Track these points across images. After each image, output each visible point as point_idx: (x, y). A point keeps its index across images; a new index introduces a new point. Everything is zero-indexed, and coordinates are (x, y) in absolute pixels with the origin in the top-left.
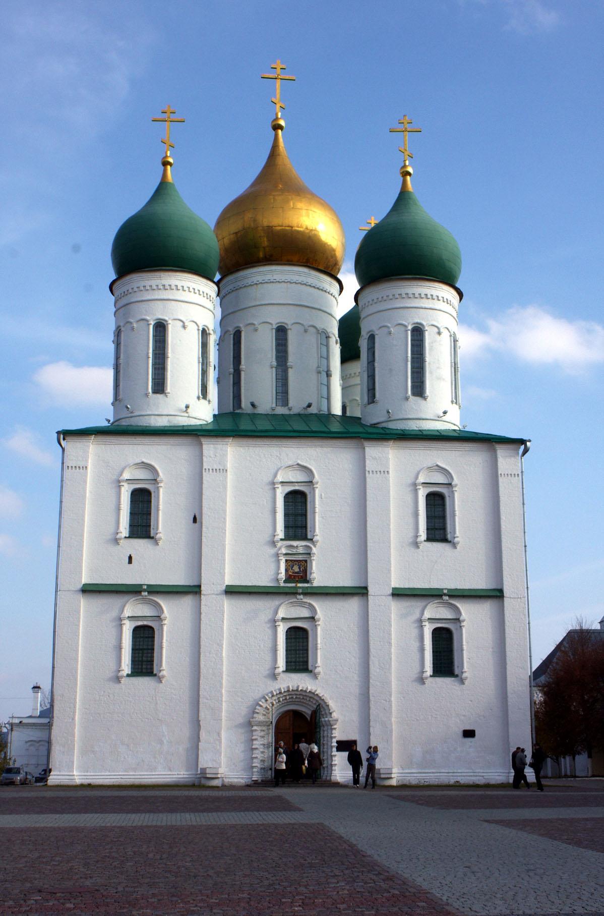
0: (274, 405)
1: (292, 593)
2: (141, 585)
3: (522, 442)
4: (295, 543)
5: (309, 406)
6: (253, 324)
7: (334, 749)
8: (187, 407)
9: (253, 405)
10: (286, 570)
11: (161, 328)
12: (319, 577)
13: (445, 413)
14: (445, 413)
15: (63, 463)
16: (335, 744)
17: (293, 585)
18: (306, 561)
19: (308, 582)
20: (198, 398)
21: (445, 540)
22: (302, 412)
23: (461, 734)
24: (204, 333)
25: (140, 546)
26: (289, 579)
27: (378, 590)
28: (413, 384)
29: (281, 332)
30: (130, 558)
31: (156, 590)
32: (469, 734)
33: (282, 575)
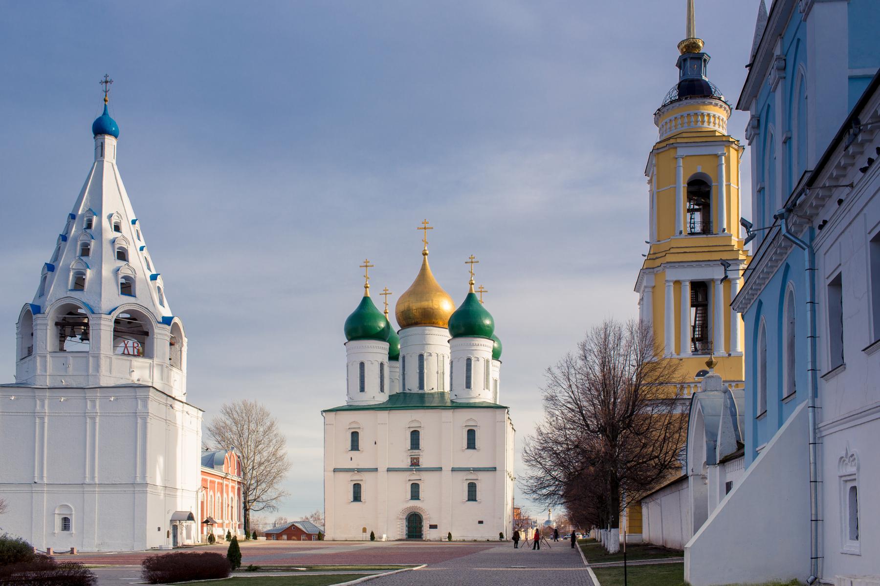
1: (411, 470)
2: (354, 469)
3: (506, 408)
4: (414, 451)
8: (374, 397)
10: (411, 462)
11: (362, 365)
12: (424, 463)
17: (413, 467)
19: (419, 466)
20: (379, 392)
21: (474, 448)
24: (382, 365)
25: (354, 454)
26: (412, 465)
27: (447, 468)
30: (351, 458)
31: (359, 470)
32: (481, 522)
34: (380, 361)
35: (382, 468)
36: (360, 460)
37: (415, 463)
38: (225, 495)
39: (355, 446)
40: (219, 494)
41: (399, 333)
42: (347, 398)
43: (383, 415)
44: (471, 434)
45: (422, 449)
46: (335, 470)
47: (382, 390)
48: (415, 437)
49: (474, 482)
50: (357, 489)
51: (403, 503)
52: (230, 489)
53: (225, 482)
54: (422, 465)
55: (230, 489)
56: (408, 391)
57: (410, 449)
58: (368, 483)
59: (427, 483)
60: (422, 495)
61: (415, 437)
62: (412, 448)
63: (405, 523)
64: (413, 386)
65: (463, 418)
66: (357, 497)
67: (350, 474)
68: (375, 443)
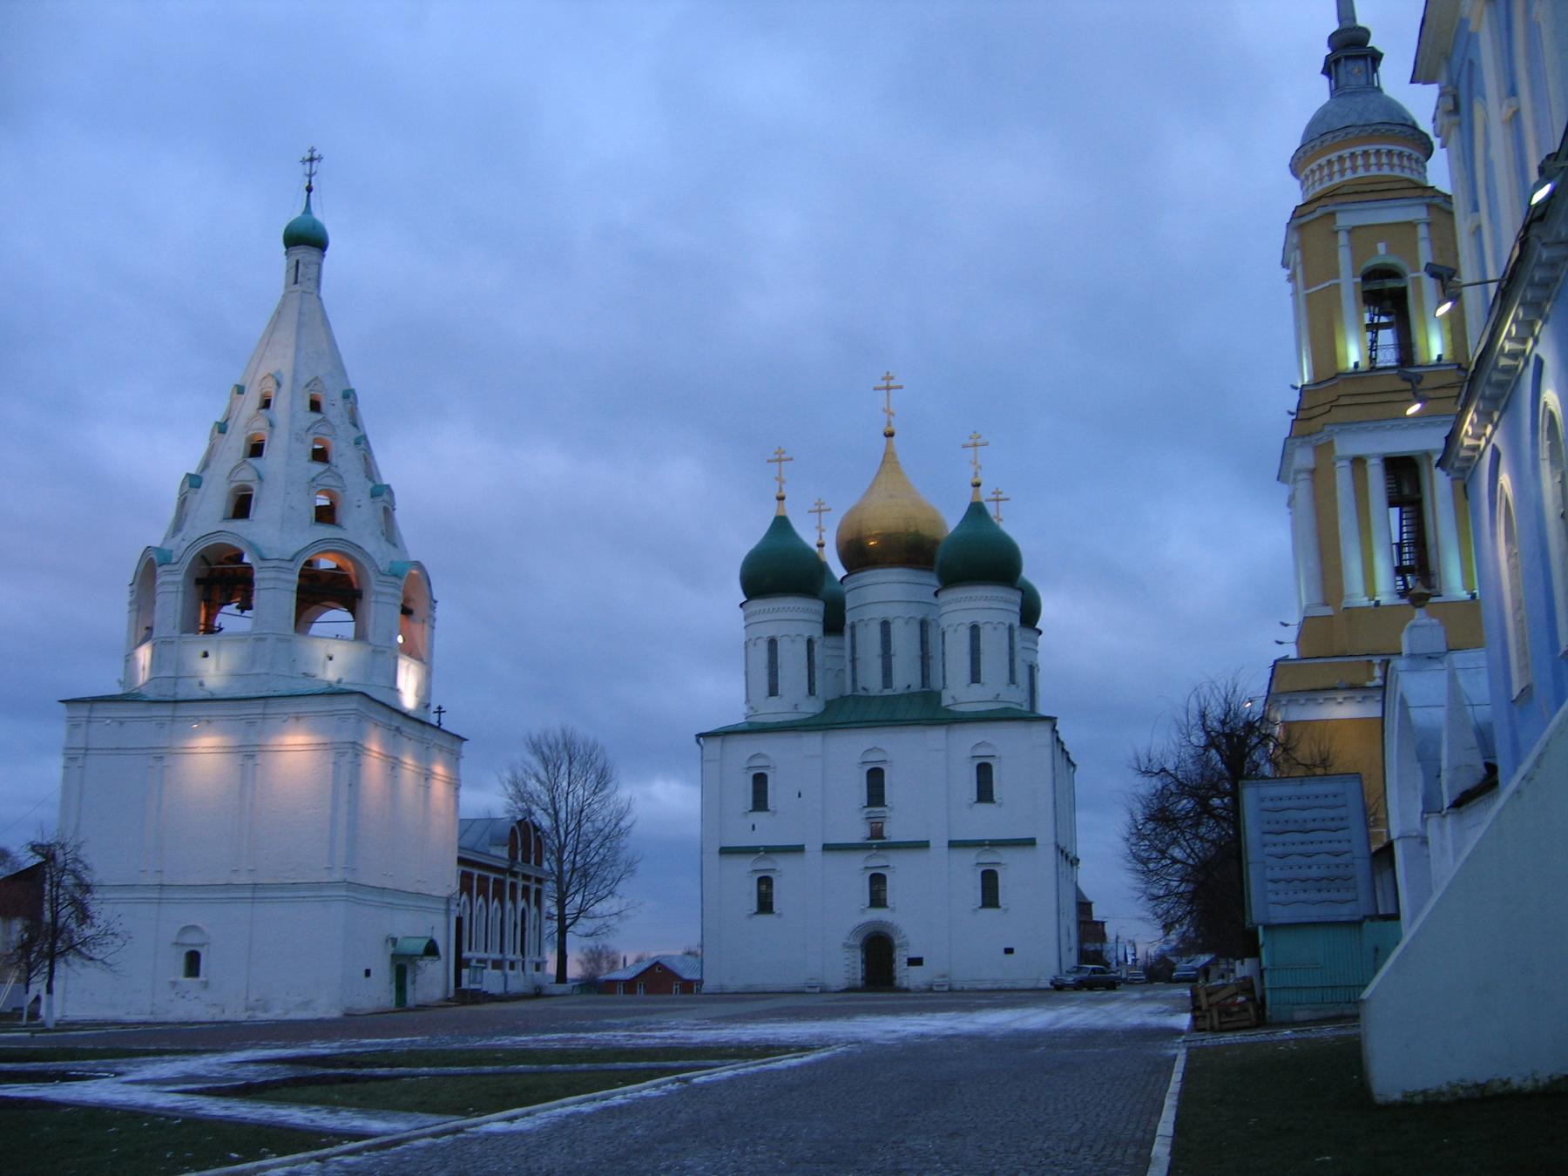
0: (881, 688)
2: (760, 847)
5: (909, 686)
6: (863, 620)
7: (906, 964)
9: (864, 689)
12: (893, 832)
13: (998, 695)
14: (998, 695)
15: (702, 758)
16: (905, 960)
18: (882, 823)
19: (884, 838)
22: (906, 692)
23: (1003, 951)
24: (810, 642)
25: (759, 818)
28: (1033, 647)
29: (885, 626)
31: (771, 850)
32: (1009, 951)
33: (868, 834)
34: (807, 635)
35: (813, 847)
36: (767, 830)
37: (877, 833)
38: (509, 905)
39: (760, 801)
40: (496, 903)
41: (844, 582)
42: (744, 709)
43: (812, 742)
44: (984, 772)
45: (890, 805)
46: (724, 851)
47: (811, 691)
48: (875, 779)
49: (992, 868)
50: (765, 882)
51: (856, 913)
52: (519, 893)
53: (509, 880)
54: (890, 837)
55: (519, 893)
56: (863, 693)
57: (866, 804)
58: (786, 873)
59: (902, 872)
60: (891, 897)
61: (875, 779)
62: (870, 804)
63: (858, 956)
64: (871, 679)
65: (966, 743)
66: (765, 905)
67: (753, 857)
68: (800, 795)
